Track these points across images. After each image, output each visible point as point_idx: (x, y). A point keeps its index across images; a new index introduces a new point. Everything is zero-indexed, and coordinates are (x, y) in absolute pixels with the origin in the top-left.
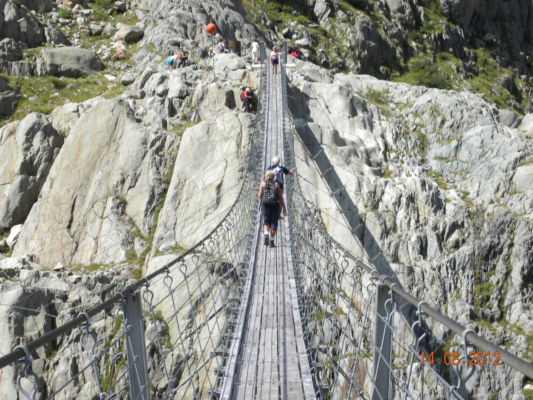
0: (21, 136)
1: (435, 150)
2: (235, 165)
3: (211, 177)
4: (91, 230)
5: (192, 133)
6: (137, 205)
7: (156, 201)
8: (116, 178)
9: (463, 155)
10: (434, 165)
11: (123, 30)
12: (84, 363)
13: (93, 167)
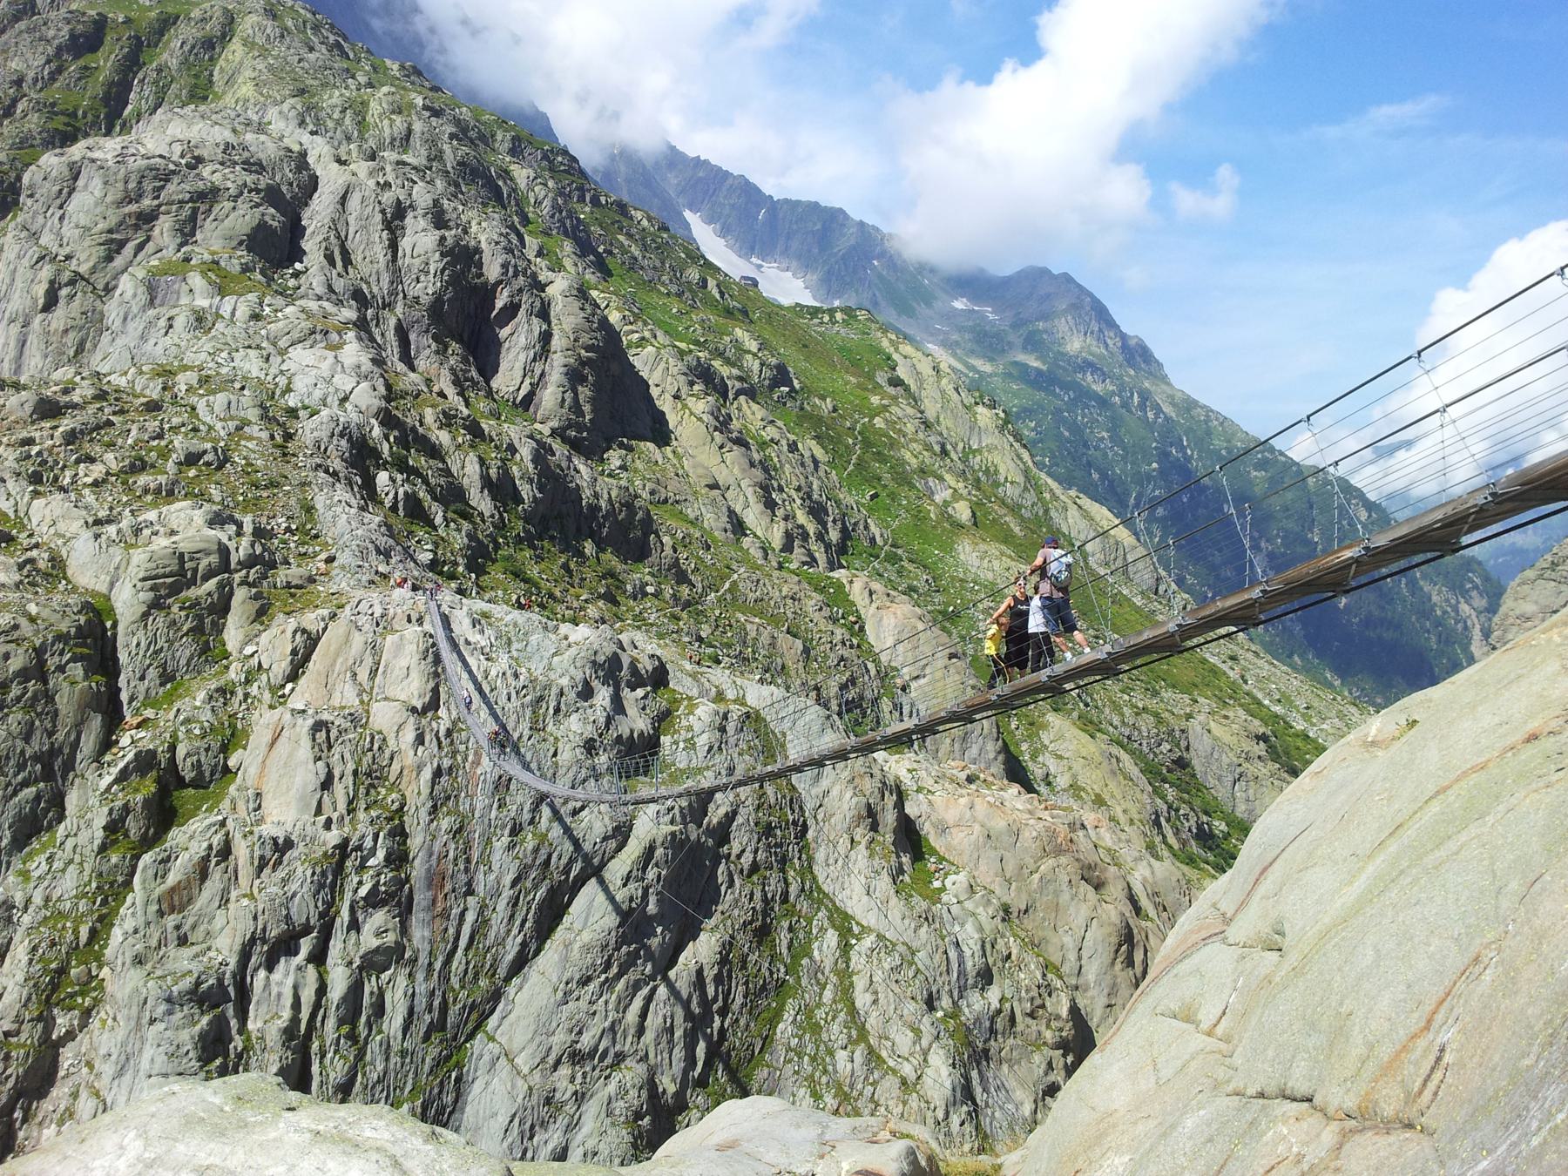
0: (289, 634)
1: (515, 646)
2: (416, 657)
3: (404, 663)
4: (339, 688)
5: (390, 639)
6: (363, 676)
7: (373, 673)
9: (529, 649)
10: (515, 654)
11: (323, 556)
12: (347, 756)
13: (337, 655)
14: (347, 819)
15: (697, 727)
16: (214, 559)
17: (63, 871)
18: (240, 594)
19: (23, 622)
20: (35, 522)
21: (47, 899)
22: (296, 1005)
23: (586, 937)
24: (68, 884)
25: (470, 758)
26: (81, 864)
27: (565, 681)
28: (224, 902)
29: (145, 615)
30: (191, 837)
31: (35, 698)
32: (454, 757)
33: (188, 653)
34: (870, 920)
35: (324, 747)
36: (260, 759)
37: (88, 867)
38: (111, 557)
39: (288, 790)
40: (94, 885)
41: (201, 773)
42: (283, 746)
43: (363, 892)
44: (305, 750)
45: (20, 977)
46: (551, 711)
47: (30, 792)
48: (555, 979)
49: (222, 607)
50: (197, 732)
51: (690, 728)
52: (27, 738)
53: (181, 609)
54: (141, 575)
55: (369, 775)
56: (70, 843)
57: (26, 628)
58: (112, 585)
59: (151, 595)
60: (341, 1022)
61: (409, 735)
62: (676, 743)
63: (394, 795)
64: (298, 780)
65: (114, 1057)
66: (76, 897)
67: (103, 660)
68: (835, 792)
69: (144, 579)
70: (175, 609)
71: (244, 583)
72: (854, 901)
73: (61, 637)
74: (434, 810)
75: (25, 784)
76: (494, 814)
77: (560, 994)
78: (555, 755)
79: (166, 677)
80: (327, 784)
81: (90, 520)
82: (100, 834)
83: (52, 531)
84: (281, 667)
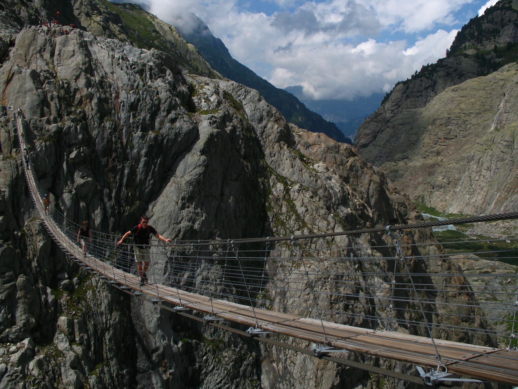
3: (70, 48)
7: (52, 55)
8: (38, 49)
13: (30, 46)
15: (208, 93)
23: (187, 178)
25: (114, 95)
27: (151, 64)
32: (105, 94)
34: (295, 178)
39: (23, 104)
42: (15, 84)
44: (29, 84)
46: (148, 76)
48: (175, 198)
51: (205, 94)
62: (200, 99)
64: (28, 99)
68: (269, 125)
72: (285, 170)
74: (101, 119)
76: (131, 121)
77: (180, 204)
78: (158, 94)
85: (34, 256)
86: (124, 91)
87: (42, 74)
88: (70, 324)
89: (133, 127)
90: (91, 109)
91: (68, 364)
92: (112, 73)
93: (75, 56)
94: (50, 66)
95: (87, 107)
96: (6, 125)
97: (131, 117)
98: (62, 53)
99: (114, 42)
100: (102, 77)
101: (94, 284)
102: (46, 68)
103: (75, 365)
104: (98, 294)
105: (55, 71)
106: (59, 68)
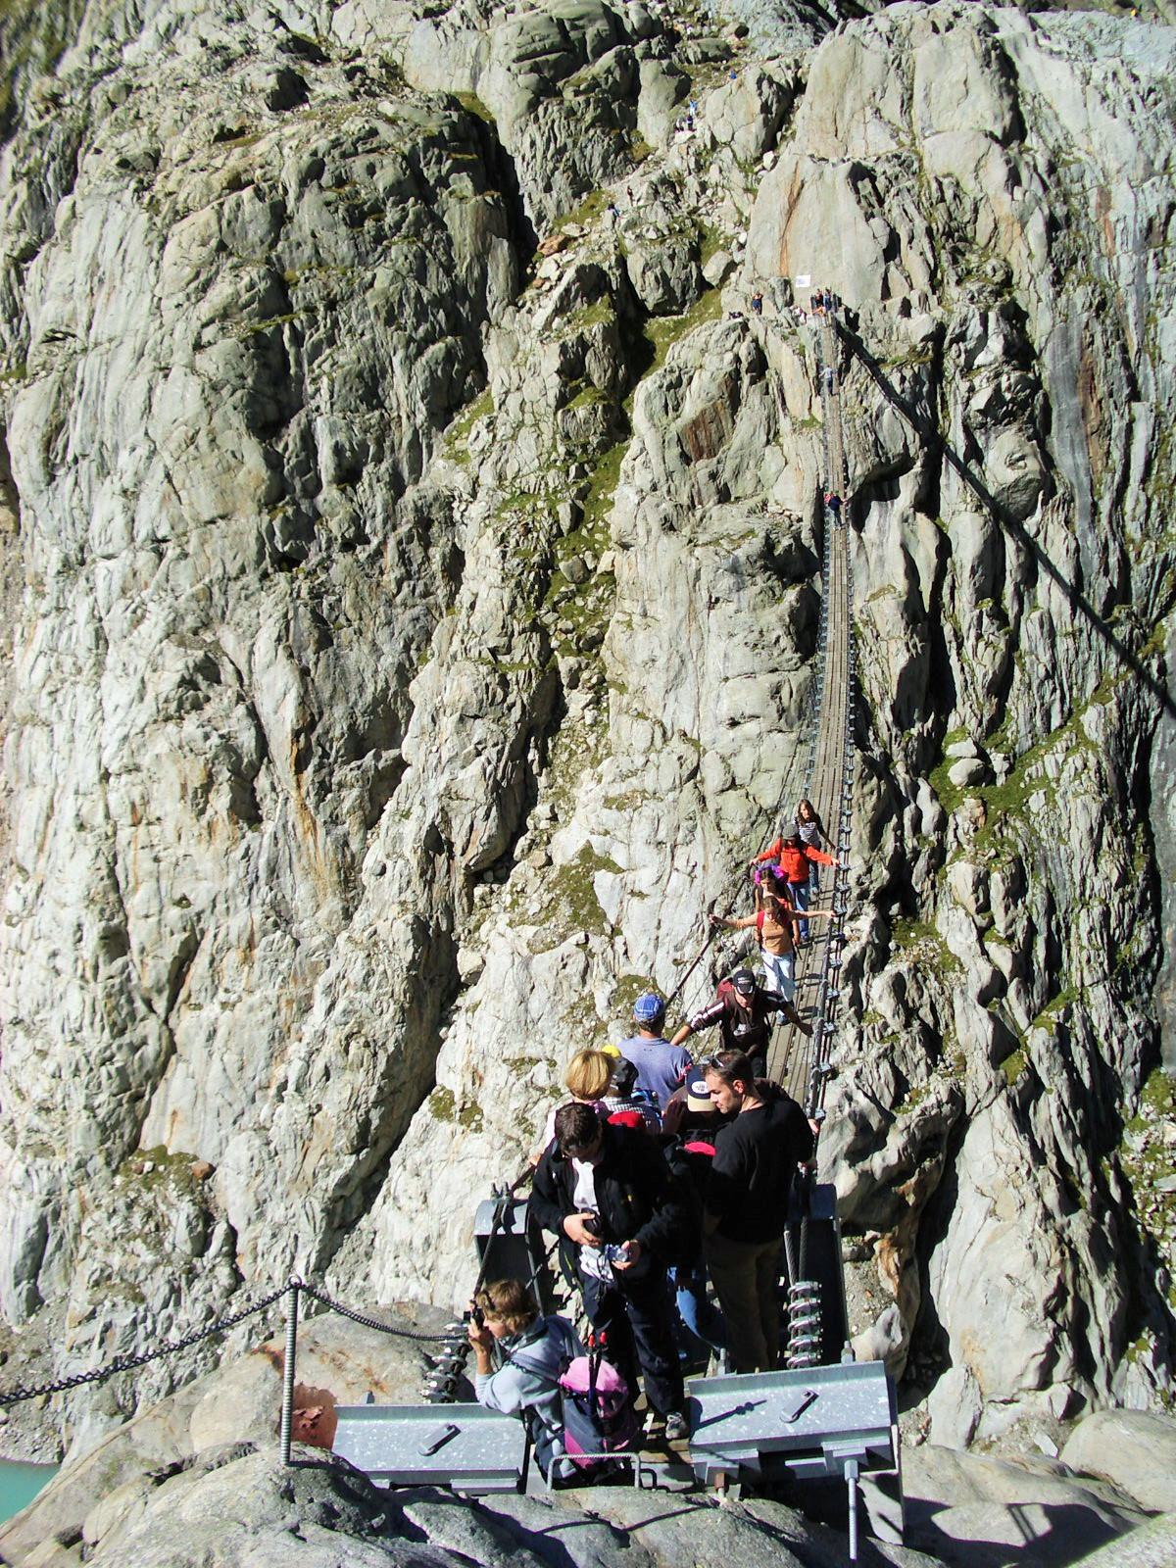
0: (751, 85)
2: (975, 65)
3: (956, 74)
6: (892, 108)
7: (907, 103)
8: (868, 93)
13: (843, 88)
14: (933, 300)
16: (601, 25)
17: (514, 437)
18: (647, 71)
19: (382, 127)
20: (343, 35)
21: (501, 477)
22: (912, 572)
24: (525, 455)
25: (1093, 200)
26: (536, 425)
28: (773, 436)
29: (533, 106)
30: (703, 352)
31: (418, 224)
33: (599, 150)
35: (873, 200)
36: (777, 235)
37: (547, 428)
38: (464, 45)
40: (562, 449)
41: (669, 290)
43: (980, 401)
44: (846, 205)
45: (495, 577)
47: (437, 349)
49: (630, 90)
50: (652, 235)
52: (421, 278)
53: (577, 93)
54: (514, 54)
55: (949, 234)
56: (513, 402)
57: (386, 133)
58: (474, 79)
59: (534, 76)
60: (980, 594)
61: (997, 171)
63: (993, 262)
64: (847, 251)
65: (661, 662)
66: (540, 468)
67: (493, 168)
69: (520, 59)
70: (568, 94)
71: (648, 55)
73: (432, 141)
74: (1058, 280)
75: (430, 339)
79: (581, 185)
80: (891, 251)
81: (420, 12)
82: (554, 381)
83: (371, 37)
84: (751, 132)
85: (884, 693)
86: (1124, 185)
87: (879, 170)
88: (981, 882)
89: (1159, 295)
90: (1025, 252)
91: (973, 993)
92: (1087, 131)
93: (972, 97)
94: (903, 137)
95: (1014, 251)
96: (794, 333)
97: (1151, 264)
98: (933, 94)
99: (1091, 25)
100: (1056, 152)
101: (1052, 773)
102: (893, 147)
103: (992, 993)
104: (1061, 803)
105: (917, 153)
106: (926, 142)
